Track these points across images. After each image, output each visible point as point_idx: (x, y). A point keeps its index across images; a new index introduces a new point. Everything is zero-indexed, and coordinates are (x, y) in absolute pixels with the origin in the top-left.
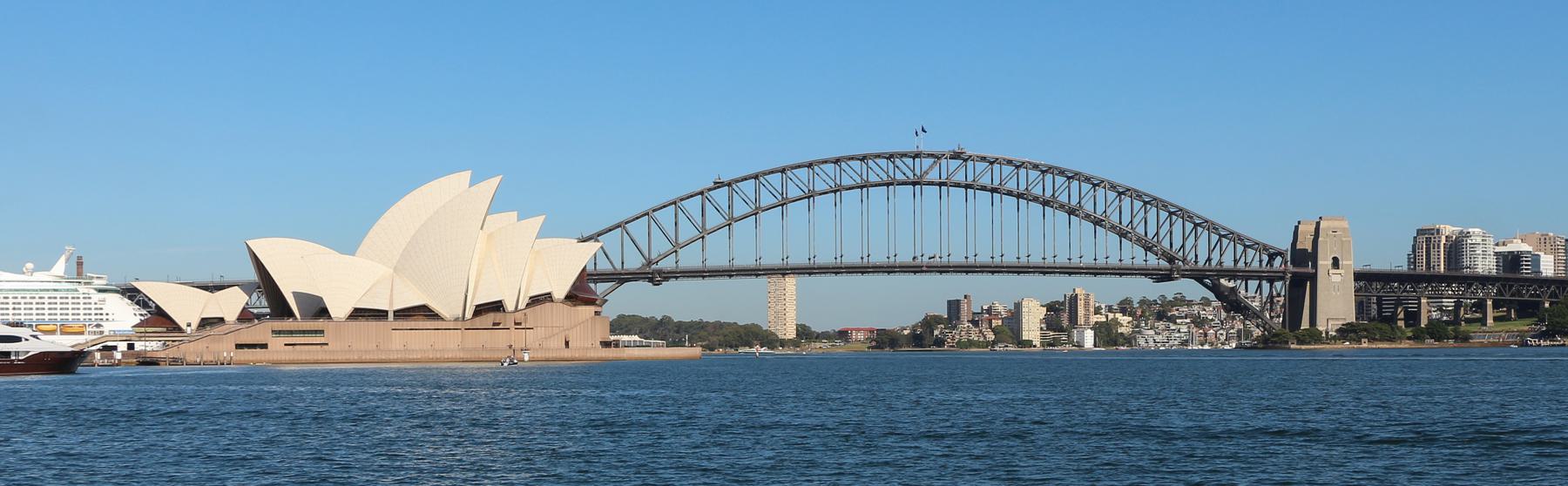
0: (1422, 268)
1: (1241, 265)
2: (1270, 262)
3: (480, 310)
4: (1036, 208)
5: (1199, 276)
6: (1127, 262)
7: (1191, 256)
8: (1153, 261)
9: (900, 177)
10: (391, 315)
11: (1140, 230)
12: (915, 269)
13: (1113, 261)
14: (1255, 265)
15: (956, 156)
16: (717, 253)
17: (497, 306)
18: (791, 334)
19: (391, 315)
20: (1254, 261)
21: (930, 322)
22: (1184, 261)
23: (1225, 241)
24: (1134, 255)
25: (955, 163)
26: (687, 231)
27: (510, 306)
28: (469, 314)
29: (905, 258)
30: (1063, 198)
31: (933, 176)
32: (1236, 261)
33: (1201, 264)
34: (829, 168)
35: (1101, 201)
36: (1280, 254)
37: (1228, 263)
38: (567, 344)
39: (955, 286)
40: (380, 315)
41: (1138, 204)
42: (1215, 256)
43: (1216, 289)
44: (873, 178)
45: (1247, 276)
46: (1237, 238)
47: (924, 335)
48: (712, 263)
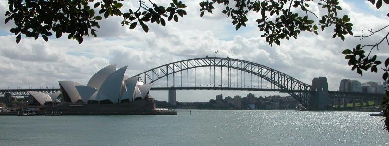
0: (343, 91)
1: (299, 89)
2: (307, 88)
3: (123, 101)
4: (247, 73)
5: (286, 91)
6: (270, 88)
7: (286, 87)
8: (277, 88)
9: (211, 64)
10: (99, 103)
11: (273, 79)
12: (215, 88)
13: (266, 88)
14: (303, 89)
15: (226, 59)
16: (163, 83)
17: (127, 100)
18: (175, 104)
19: (99, 103)
20: (303, 88)
21: (212, 101)
22: (285, 87)
23: (295, 83)
24: (271, 86)
25: (225, 61)
26: (155, 77)
27: (131, 100)
28: (120, 101)
29: (212, 86)
30: (254, 71)
31: (220, 64)
32: (298, 88)
33: (289, 89)
34: (193, 61)
35: (263, 71)
36: (309, 86)
37: (296, 88)
38: (145, 110)
39: (219, 92)
40: (97, 101)
41: (273, 73)
42: (293, 86)
43: (294, 96)
44: (204, 64)
45: (300, 91)
46: (298, 82)
47: (212, 105)
48: (162, 86)
